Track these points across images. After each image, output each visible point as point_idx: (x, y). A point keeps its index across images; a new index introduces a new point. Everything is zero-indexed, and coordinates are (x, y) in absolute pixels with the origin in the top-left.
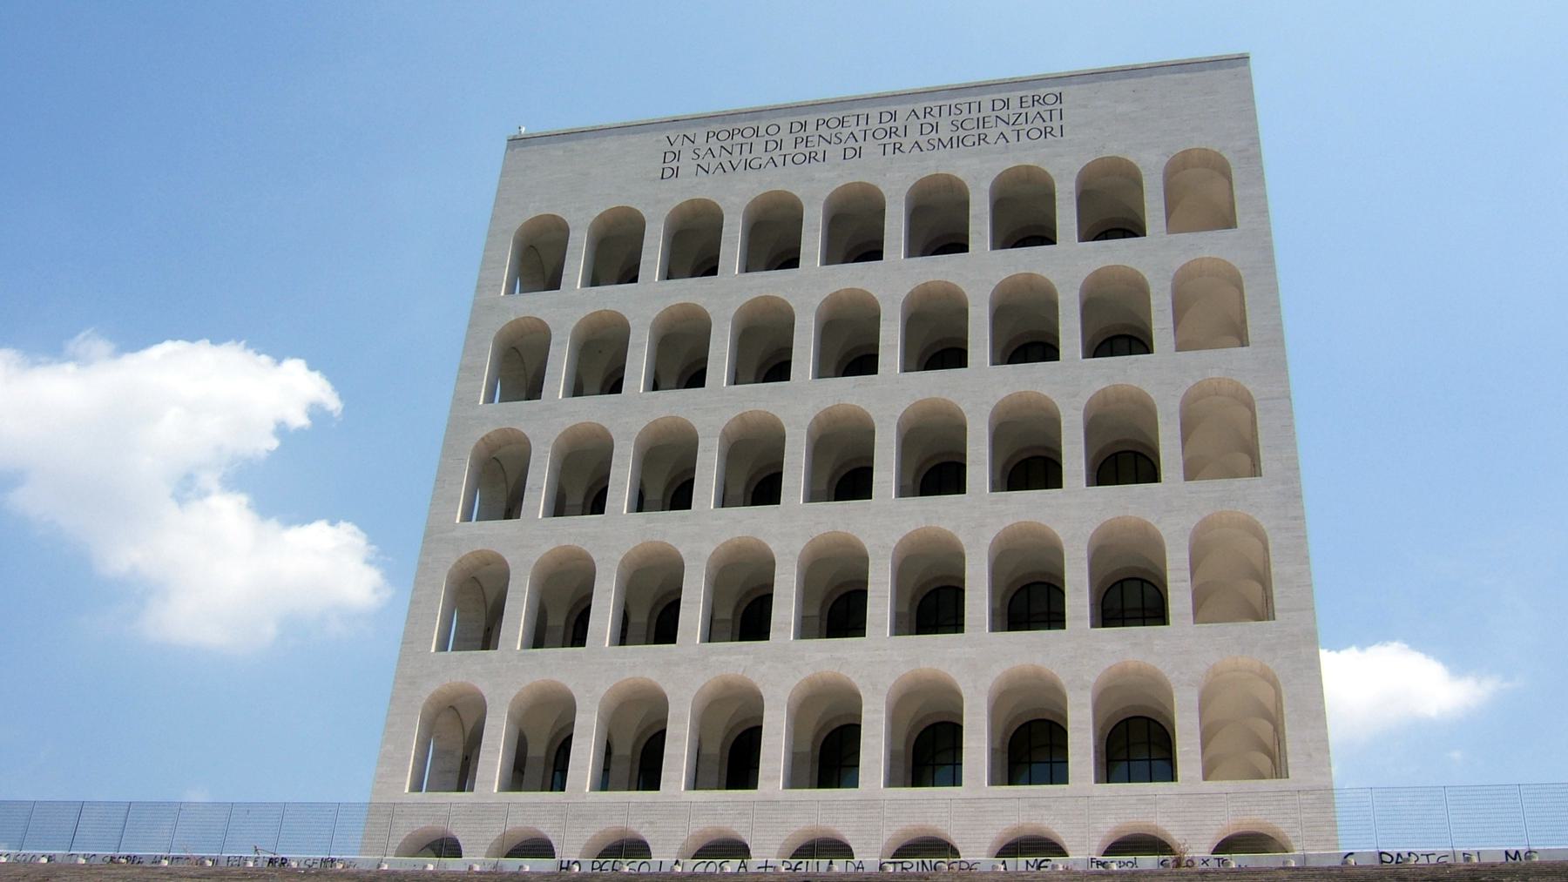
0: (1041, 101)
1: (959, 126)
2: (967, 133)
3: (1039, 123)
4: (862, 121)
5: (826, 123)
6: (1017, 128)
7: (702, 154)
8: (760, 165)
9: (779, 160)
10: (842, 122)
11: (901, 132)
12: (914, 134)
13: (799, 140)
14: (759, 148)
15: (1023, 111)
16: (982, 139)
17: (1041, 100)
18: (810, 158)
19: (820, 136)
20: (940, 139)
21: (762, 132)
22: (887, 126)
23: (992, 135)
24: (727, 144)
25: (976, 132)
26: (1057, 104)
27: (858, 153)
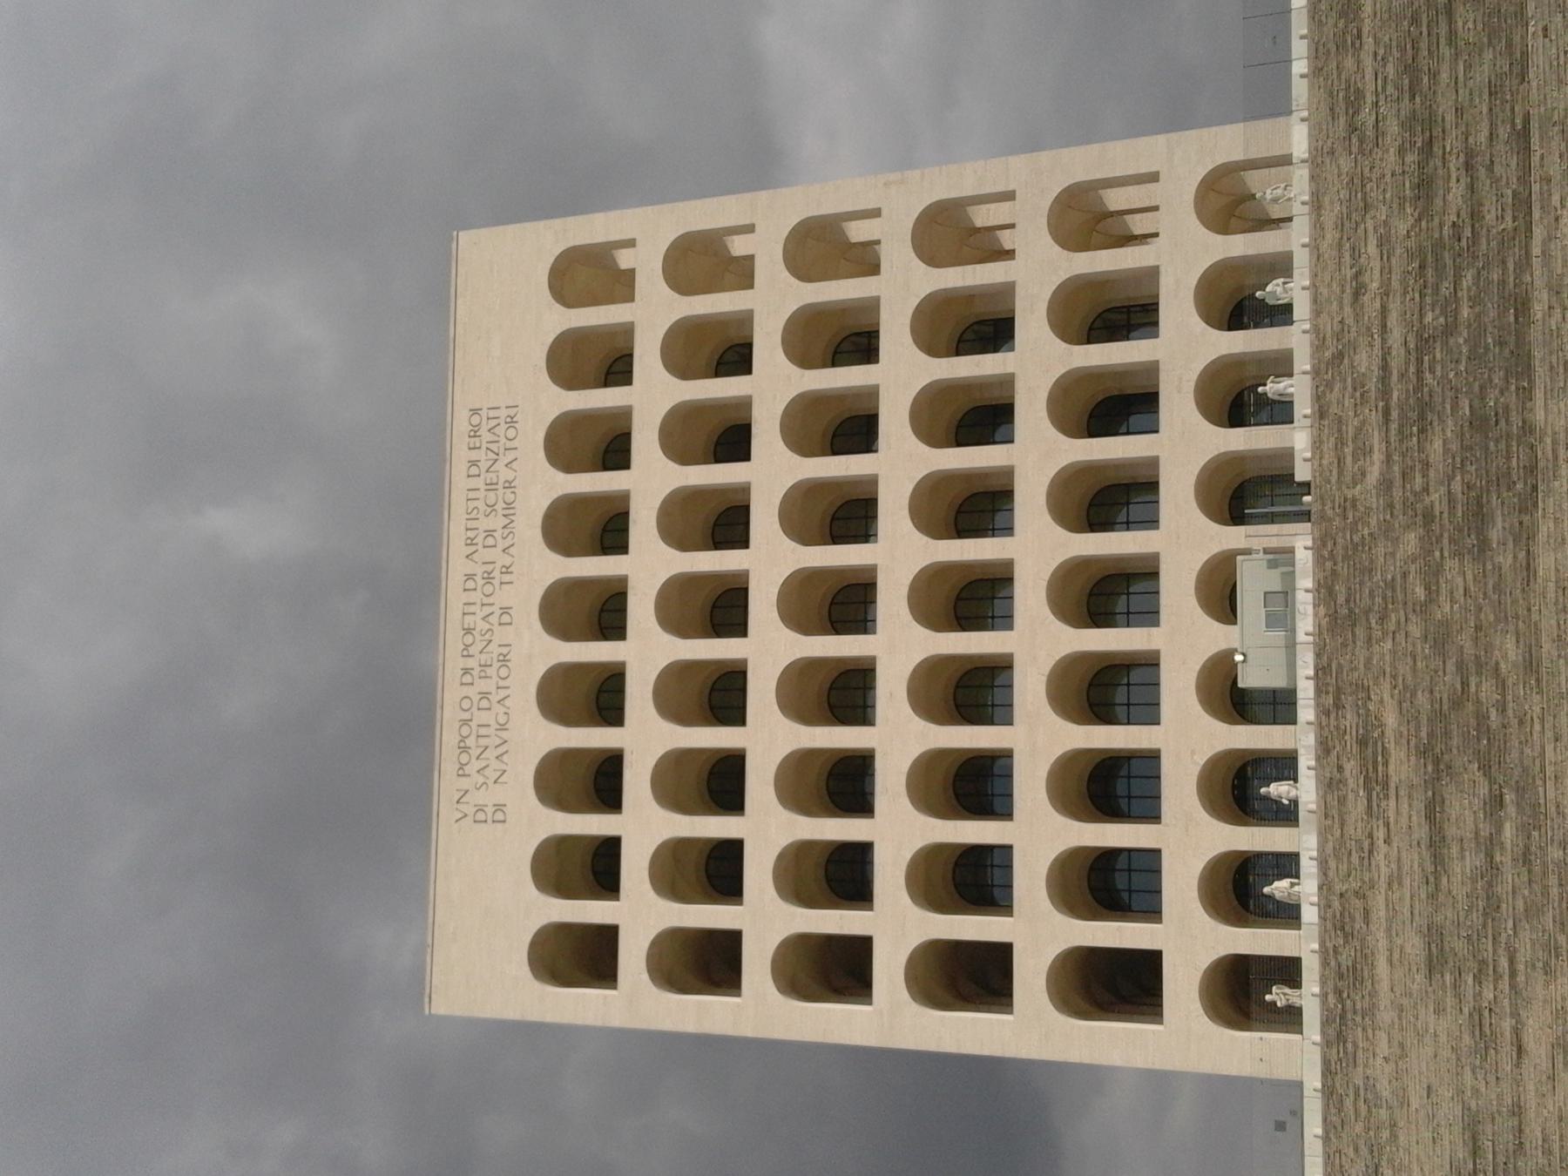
0: (476, 429)
1: (492, 509)
2: (500, 499)
3: (500, 430)
4: (472, 609)
5: (467, 647)
6: (502, 450)
7: (481, 780)
8: (506, 713)
9: (503, 693)
10: (468, 631)
11: (490, 568)
12: (495, 554)
13: (483, 674)
14: (483, 717)
15: (484, 446)
16: (509, 485)
18: (504, 660)
19: (481, 653)
20: (504, 527)
21: (466, 716)
22: (481, 582)
23: (506, 474)
24: (475, 752)
25: (501, 491)
26: (484, 413)
27: (505, 610)
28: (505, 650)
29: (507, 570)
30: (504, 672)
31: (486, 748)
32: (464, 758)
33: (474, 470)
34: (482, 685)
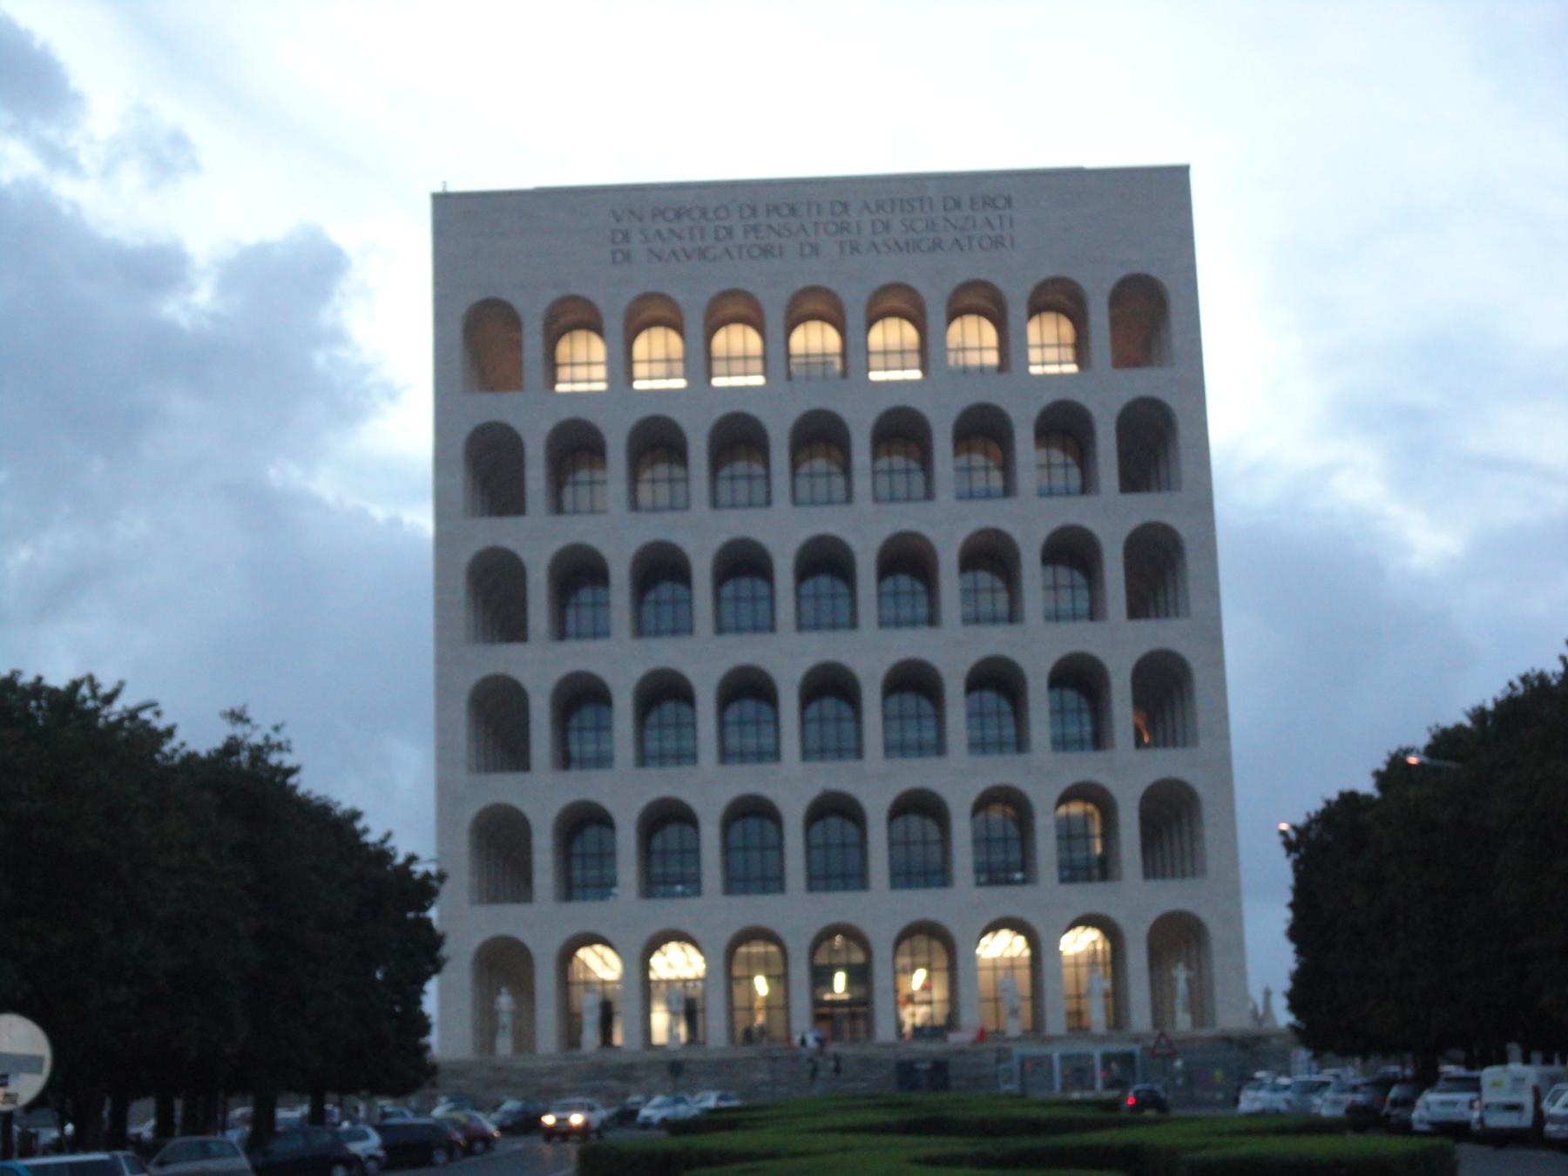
5: (777, 208)
9: (735, 253)
10: (793, 211)
17: (989, 202)
18: (766, 252)
19: (770, 227)
20: (897, 243)
21: (711, 215)
27: (816, 250)
28: (776, 252)
29: (855, 248)
30: (756, 252)
31: (680, 238)
32: (670, 215)
33: (950, 204)
34: (739, 231)
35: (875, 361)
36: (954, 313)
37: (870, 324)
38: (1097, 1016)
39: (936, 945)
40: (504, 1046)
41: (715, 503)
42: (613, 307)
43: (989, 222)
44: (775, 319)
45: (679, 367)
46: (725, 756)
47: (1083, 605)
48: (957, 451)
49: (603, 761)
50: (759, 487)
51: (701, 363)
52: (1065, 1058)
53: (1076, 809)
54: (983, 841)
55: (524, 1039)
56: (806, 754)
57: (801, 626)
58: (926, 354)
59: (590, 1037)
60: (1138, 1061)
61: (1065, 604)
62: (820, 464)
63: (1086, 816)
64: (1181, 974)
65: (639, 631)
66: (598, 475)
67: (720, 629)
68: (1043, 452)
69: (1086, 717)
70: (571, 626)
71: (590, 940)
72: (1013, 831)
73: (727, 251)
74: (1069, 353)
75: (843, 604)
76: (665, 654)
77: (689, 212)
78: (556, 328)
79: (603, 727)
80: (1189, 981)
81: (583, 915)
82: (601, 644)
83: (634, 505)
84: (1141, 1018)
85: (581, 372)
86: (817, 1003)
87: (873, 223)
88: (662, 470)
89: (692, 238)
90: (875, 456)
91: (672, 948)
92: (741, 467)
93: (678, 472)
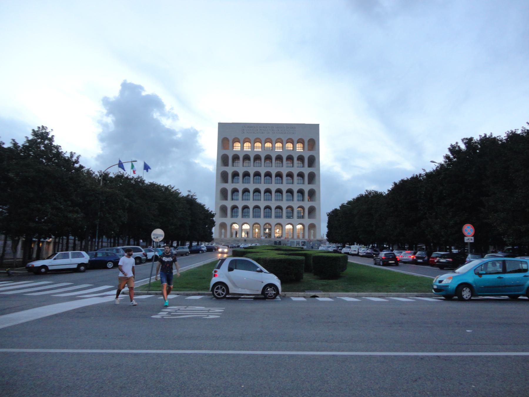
9: (258, 133)
10: (266, 127)
17: (292, 128)
18: (262, 133)
20: (280, 133)
26: (295, 129)
27: (269, 133)
30: (261, 133)
31: (251, 130)
32: (250, 127)
33: (287, 128)
34: (259, 130)
35: (276, 148)
36: (287, 142)
37: (276, 143)
38: (301, 236)
39: (280, 226)
40: (223, 236)
41: (254, 166)
42: (242, 139)
43: (292, 130)
44: (263, 142)
45: (250, 148)
46: (253, 200)
47: (302, 182)
48: (286, 161)
49: (237, 200)
50: (260, 164)
51: (253, 147)
52: (296, 241)
53: (300, 209)
54: (287, 213)
55: (225, 236)
56: (264, 200)
57: (264, 183)
58: (283, 147)
59: (234, 236)
60: (306, 243)
61: (300, 182)
62: (268, 162)
63: (301, 210)
64: (312, 231)
65: (243, 183)
66: (238, 162)
67: (254, 183)
68: (298, 161)
69: (302, 197)
70: (234, 182)
71: (235, 223)
72: (291, 212)
73: (257, 133)
74: (302, 148)
75: (270, 180)
76: (246, 186)
77: (252, 127)
78: (234, 142)
79: (238, 195)
80: (313, 232)
81: (234, 220)
82: (238, 184)
83: (243, 166)
84: (307, 237)
85: (237, 148)
86: (264, 233)
87: (277, 130)
88: (247, 161)
89: (253, 130)
90: (276, 161)
91: (245, 225)
92: (258, 161)
93: (249, 162)
